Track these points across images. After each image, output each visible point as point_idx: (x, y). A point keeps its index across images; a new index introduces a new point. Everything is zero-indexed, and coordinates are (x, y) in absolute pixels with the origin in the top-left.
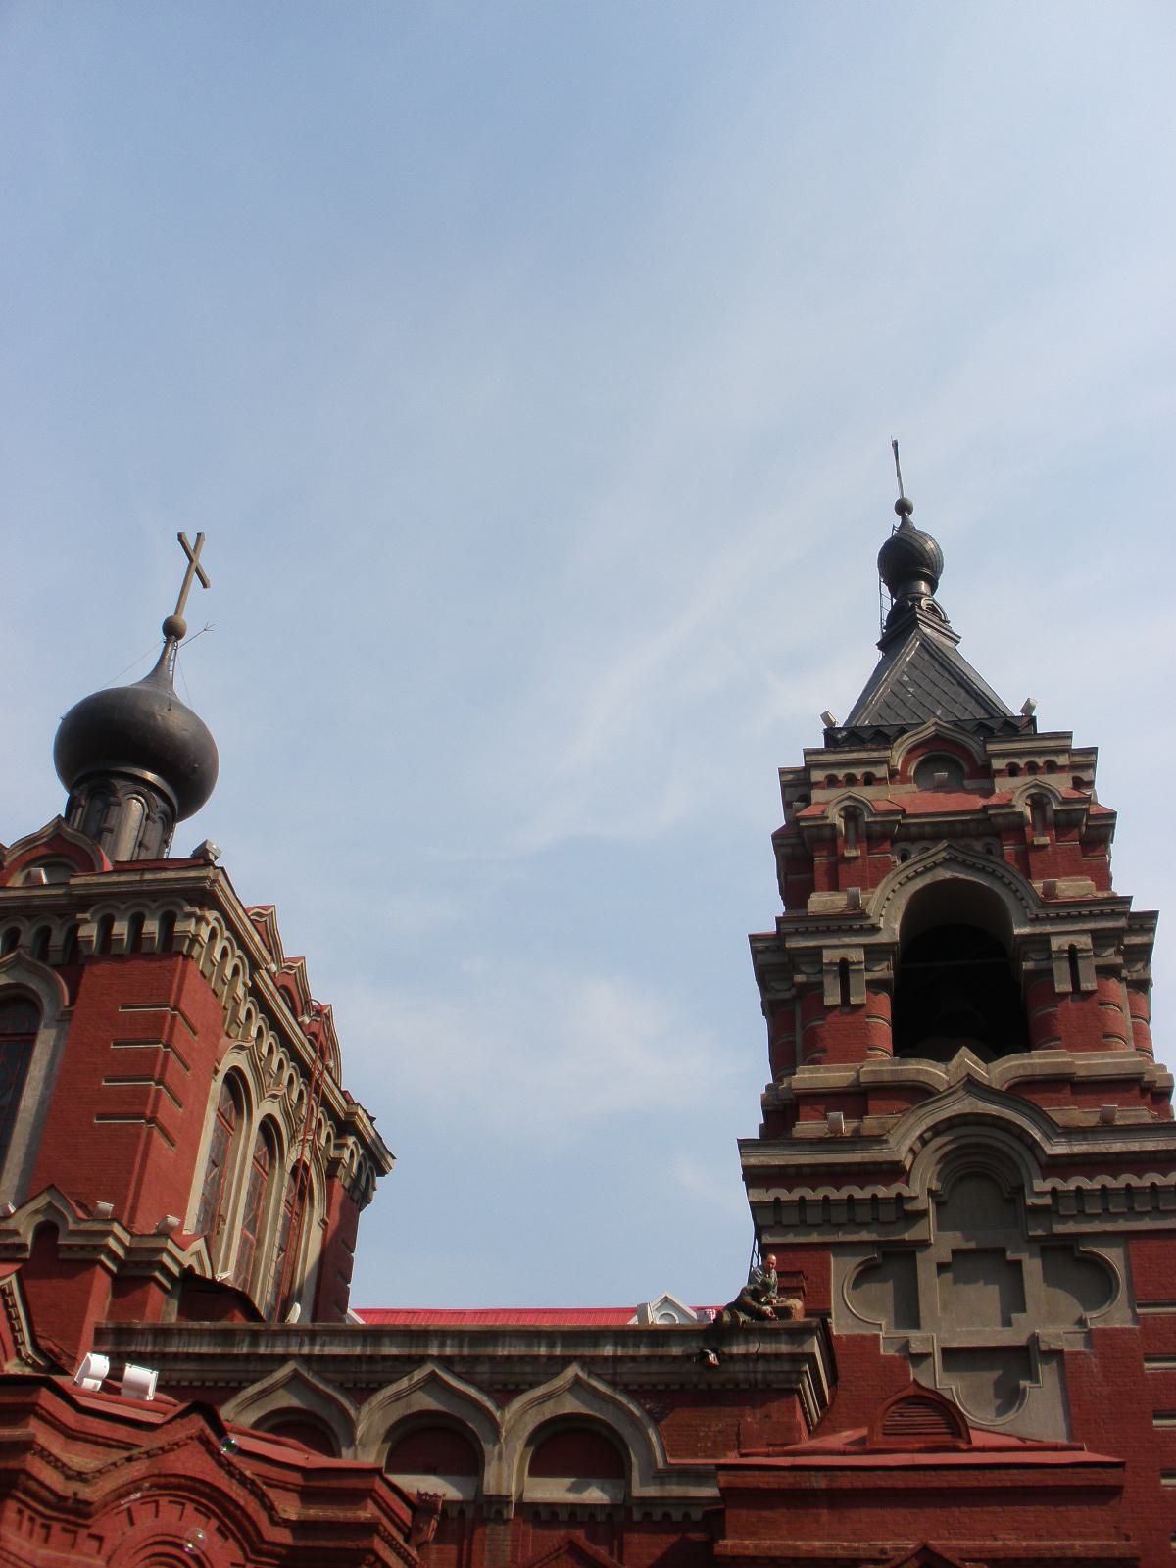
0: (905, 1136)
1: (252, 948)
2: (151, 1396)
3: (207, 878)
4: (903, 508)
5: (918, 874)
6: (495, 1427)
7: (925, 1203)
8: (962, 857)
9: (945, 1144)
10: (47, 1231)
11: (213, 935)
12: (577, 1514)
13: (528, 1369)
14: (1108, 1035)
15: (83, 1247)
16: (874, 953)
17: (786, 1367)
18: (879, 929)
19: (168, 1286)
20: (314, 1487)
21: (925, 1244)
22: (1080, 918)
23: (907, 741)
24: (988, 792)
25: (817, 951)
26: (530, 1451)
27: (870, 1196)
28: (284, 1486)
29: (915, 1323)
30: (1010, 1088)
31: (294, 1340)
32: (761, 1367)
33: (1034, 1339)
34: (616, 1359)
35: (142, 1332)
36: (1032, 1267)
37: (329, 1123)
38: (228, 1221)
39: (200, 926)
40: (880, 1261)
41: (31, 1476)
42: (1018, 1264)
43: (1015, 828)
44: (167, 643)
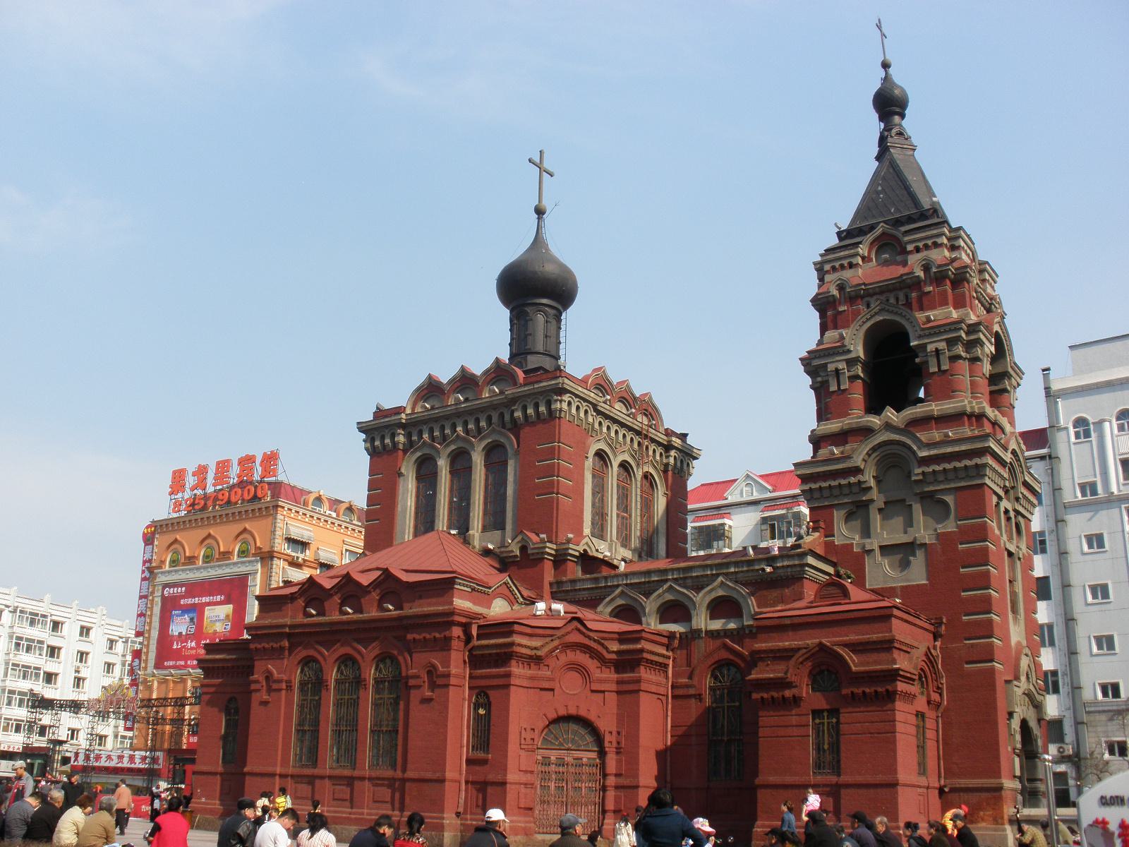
0: (860, 454)
1: (591, 400)
2: (562, 613)
5: (868, 320)
6: (694, 603)
7: (872, 483)
8: (887, 307)
9: (877, 456)
10: (524, 549)
11: (569, 403)
12: (726, 633)
13: (705, 579)
14: (953, 392)
15: (538, 553)
16: (851, 363)
17: (798, 569)
18: (851, 351)
19: (576, 560)
20: (623, 637)
21: (872, 501)
22: (940, 333)
23: (870, 237)
24: (905, 264)
25: (825, 365)
26: (709, 612)
27: (857, 481)
28: (612, 639)
29: (869, 537)
30: (906, 426)
31: (620, 579)
32: (789, 570)
33: (915, 538)
34: (736, 573)
35: (566, 582)
36: (917, 508)
37: (659, 448)
38: (609, 515)
39: (562, 404)
40: (854, 510)
41: (516, 652)
42: (911, 505)
43: (916, 284)
44: (538, 218)
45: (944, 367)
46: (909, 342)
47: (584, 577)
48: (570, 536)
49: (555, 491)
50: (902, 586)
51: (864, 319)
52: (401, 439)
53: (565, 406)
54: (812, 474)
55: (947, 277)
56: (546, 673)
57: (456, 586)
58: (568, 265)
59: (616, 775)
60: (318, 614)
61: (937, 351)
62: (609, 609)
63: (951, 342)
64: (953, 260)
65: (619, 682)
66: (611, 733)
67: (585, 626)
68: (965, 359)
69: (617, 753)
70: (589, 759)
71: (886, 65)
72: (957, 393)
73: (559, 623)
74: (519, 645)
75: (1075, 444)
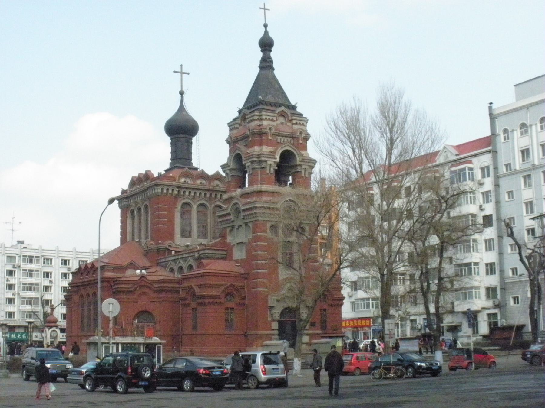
11: (162, 189)
22: (249, 159)
45: (251, 173)
48: (160, 242)
50: (241, 259)
53: (160, 191)
56: (135, 296)
61: (249, 166)
62: (169, 269)
63: (252, 162)
64: (260, 126)
71: (266, 26)
73: (138, 278)
75: (503, 143)
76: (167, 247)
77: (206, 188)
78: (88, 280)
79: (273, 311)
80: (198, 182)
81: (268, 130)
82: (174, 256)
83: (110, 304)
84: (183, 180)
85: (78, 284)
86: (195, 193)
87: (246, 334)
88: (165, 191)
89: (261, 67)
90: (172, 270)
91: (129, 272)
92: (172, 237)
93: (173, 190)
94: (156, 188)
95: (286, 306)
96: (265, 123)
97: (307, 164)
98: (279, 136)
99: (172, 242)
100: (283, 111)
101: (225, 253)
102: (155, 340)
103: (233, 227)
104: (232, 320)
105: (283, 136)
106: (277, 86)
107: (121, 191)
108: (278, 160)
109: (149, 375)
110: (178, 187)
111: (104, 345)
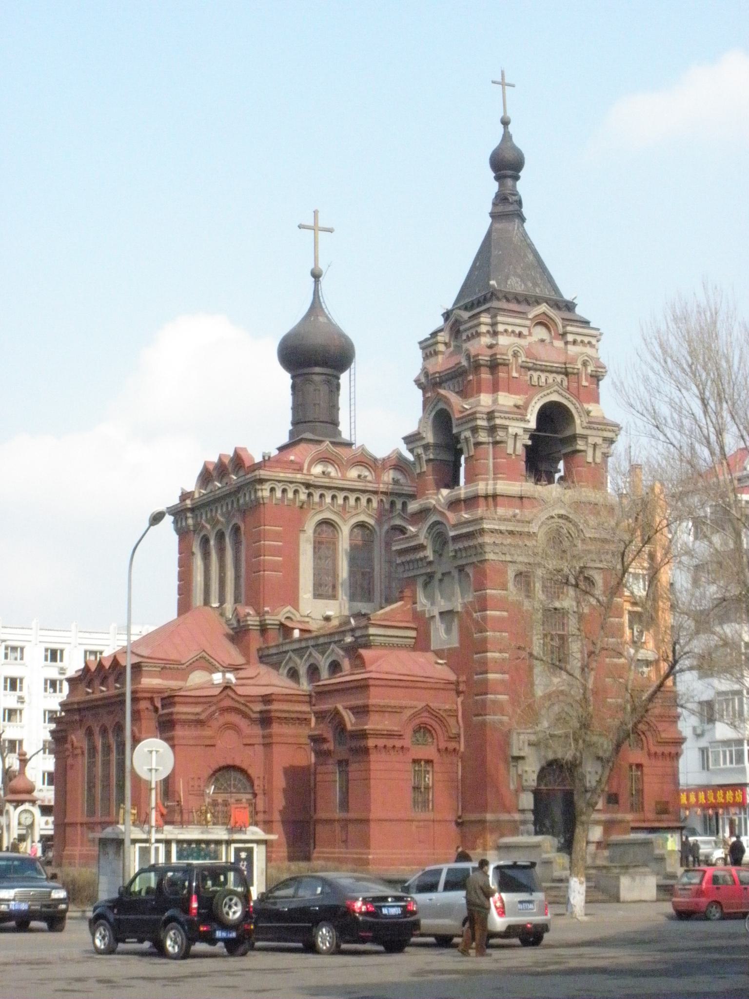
3: (255, 476)
4: (505, 123)
11: (272, 490)
14: (476, 475)
16: (426, 447)
45: (472, 453)
46: (450, 430)
47: (284, 642)
48: (266, 609)
49: (262, 569)
50: (449, 649)
51: (431, 408)
52: (190, 521)
53: (266, 493)
54: (401, 549)
55: (479, 366)
56: (208, 732)
57: (144, 669)
58: (341, 327)
59: (265, 812)
60: (93, 693)
61: (466, 439)
62: (286, 671)
63: (475, 430)
64: (491, 347)
65: (264, 737)
66: (259, 778)
67: (234, 691)
68: (489, 443)
69: (264, 794)
70: (247, 800)
72: (480, 476)
73: (216, 691)
74: (178, 713)
76: (283, 620)
77: (370, 486)
78: (106, 694)
79: (522, 767)
80: (353, 473)
81: (510, 357)
82: (300, 640)
83: (151, 752)
84: (318, 469)
85: (82, 706)
86: (346, 498)
87: (460, 821)
88: (279, 494)
89: (493, 215)
90: (293, 674)
91: (197, 678)
92: (294, 601)
93: (296, 492)
94: (258, 487)
95: (551, 756)
96: (503, 340)
97: (600, 433)
98: (536, 370)
99: (292, 610)
100: (544, 313)
101: (413, 634)
102: (253, 833)
103: (430, 576)
104: (427, 788)
105: (542, 371)
106: (531, 257)
107: (179, 494)
108: (533, 425)
109: (238, 915)
110: (308, 486)
111: (138, 845)
